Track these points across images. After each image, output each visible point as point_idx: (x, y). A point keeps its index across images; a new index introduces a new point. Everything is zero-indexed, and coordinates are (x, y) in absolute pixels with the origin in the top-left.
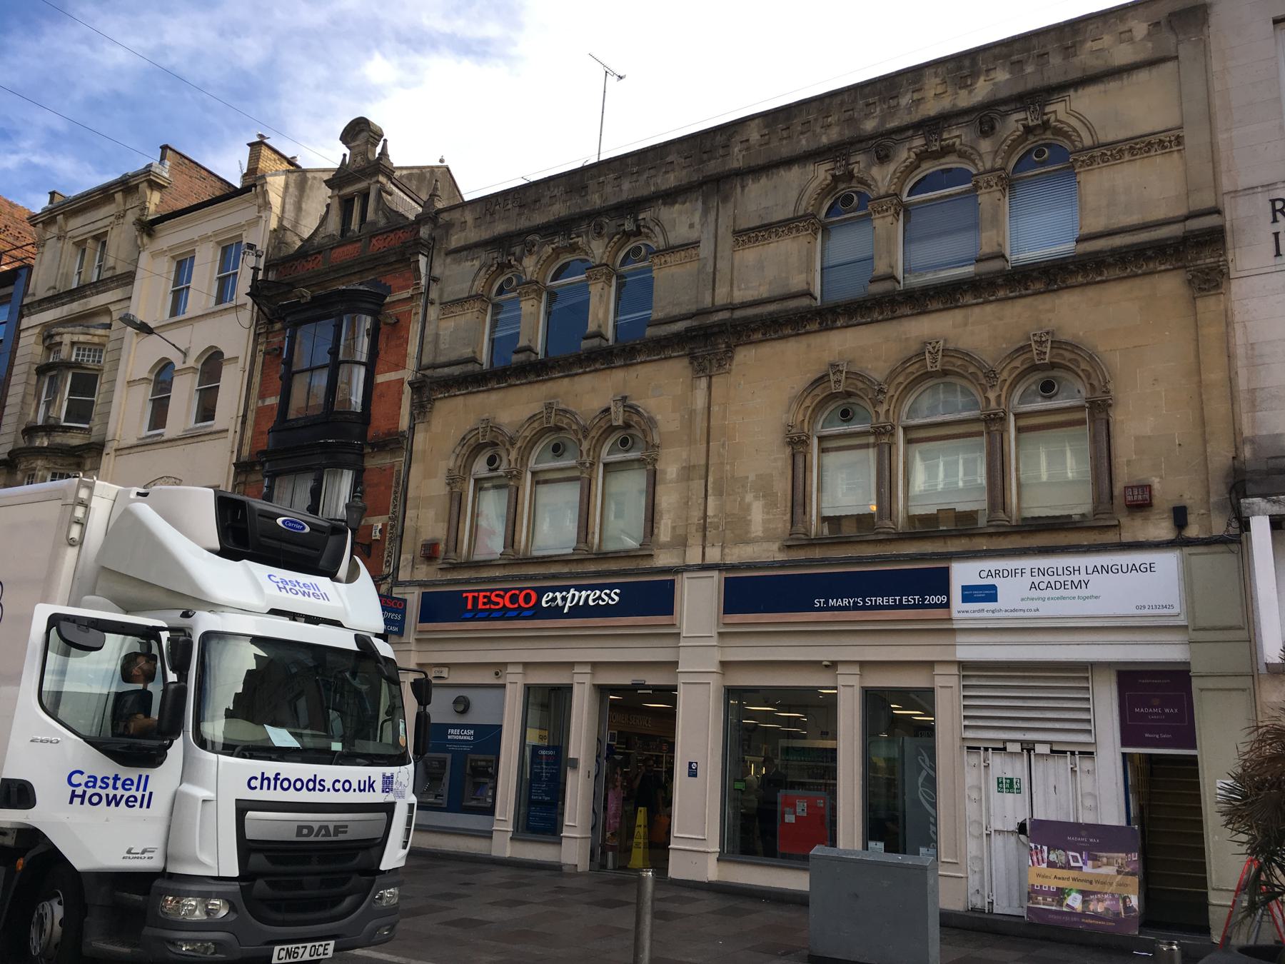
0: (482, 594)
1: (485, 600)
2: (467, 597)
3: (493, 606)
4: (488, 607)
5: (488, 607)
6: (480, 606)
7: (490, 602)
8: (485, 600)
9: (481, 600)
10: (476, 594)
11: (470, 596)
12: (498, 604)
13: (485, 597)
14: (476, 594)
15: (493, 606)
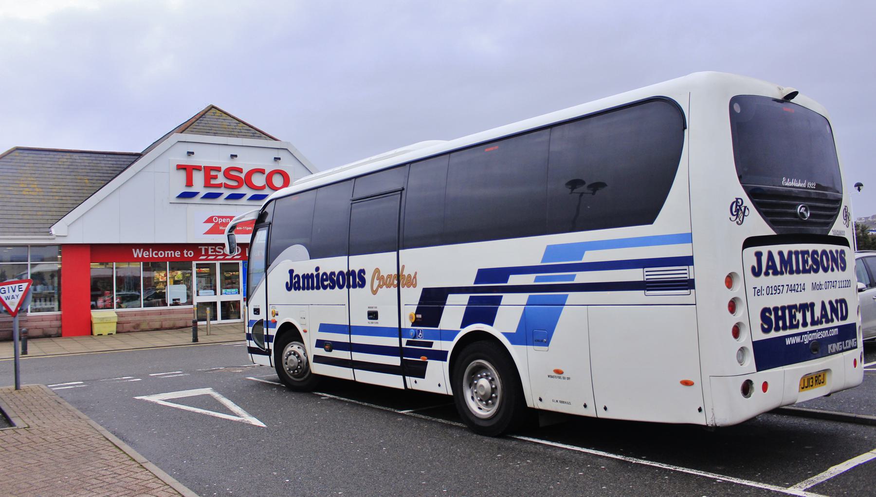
0: (210, 248)
1: (213, 250)
2: (201, 249)
3: (217, 253)
4: (214, 253)
5: (214, 253)
6: (210, 253)
7: (215, 251)
8: (213, 250)
9: (210, 251)
10: (207, 247)
11: (203, 248)
12: (220, 252)
13: (212, 249)
14: (207, 247)
15: (217, 253)
